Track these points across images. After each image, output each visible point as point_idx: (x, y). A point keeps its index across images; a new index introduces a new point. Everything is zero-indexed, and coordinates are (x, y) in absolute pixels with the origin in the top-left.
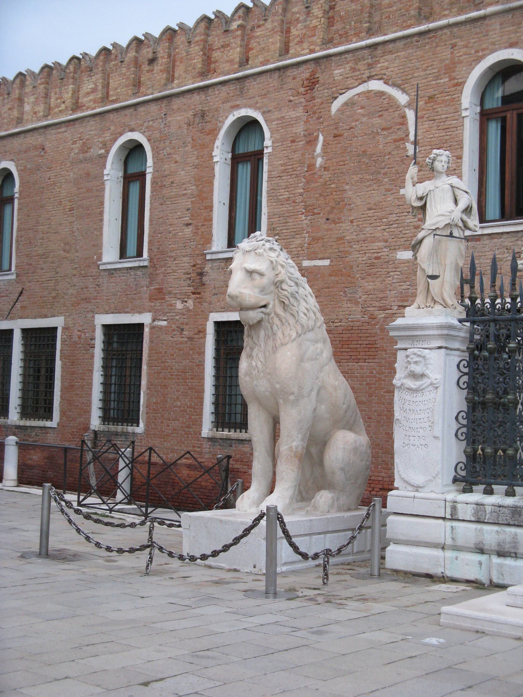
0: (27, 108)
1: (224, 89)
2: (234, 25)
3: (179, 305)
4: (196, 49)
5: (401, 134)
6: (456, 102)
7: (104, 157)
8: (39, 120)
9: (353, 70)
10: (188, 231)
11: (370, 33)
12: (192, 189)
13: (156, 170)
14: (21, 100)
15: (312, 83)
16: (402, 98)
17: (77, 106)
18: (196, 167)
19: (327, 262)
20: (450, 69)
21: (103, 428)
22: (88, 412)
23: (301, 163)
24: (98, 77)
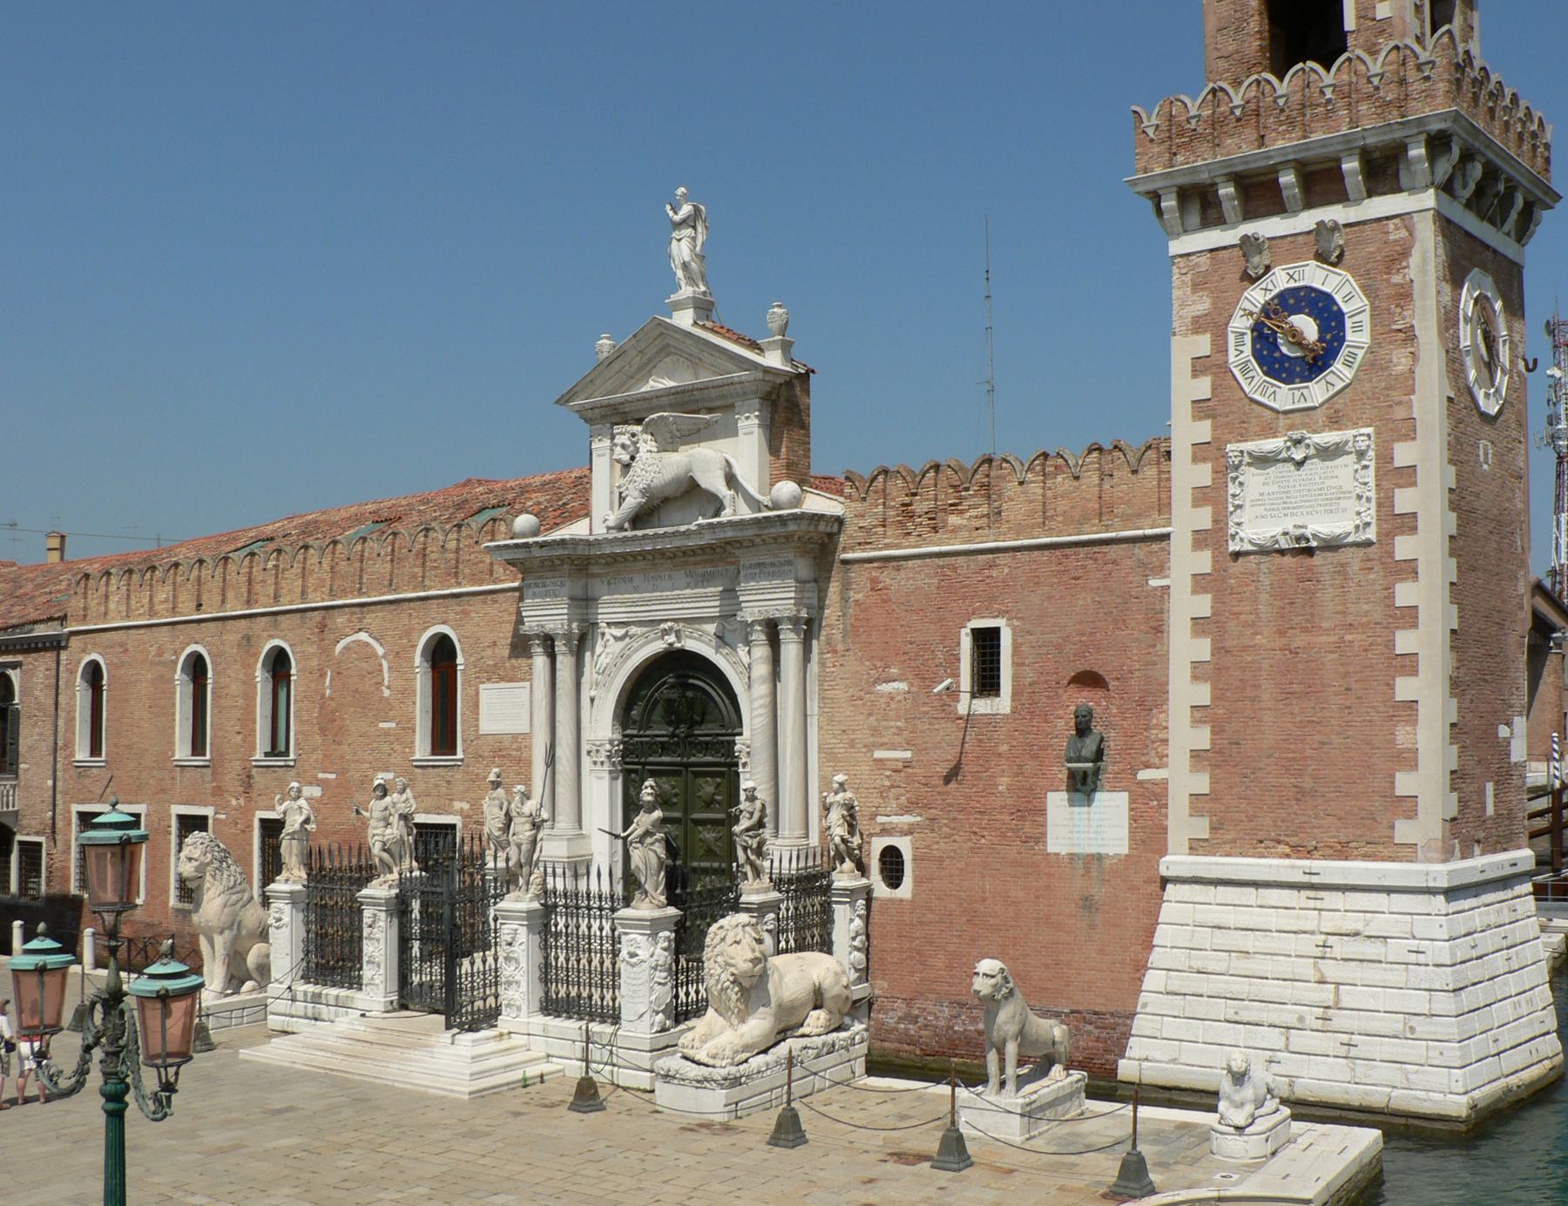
0: (112, 606)
1: (264, 619)
2: (270, 564)
3: (234, 802)
4: (243, 579)
5: (378, 679)
6: (411, 660)
7: (175, 663)
8: (122, 619)
9: (350, 621)
10: (239, 737)
11: (360, 593)
12: (241, 702)
13: (215, 682)
14: (107, 596)
15: (323, 628)
16: (380, 651)
17: (152, 612)
18: (244, 683)
19: (333, 776)
20: (408, 633)
21: (180, 905)
22: (167, 891)
23: (316, 691)
24: (168, 588)
